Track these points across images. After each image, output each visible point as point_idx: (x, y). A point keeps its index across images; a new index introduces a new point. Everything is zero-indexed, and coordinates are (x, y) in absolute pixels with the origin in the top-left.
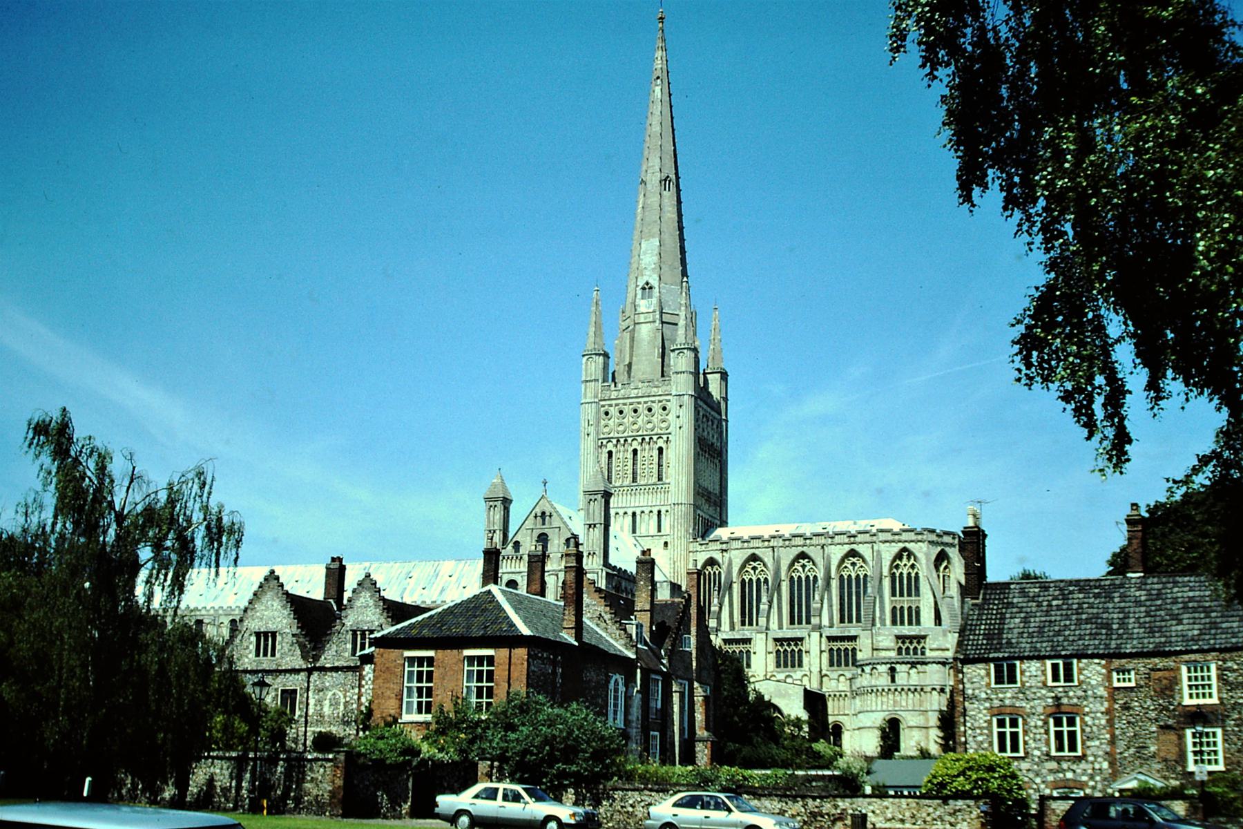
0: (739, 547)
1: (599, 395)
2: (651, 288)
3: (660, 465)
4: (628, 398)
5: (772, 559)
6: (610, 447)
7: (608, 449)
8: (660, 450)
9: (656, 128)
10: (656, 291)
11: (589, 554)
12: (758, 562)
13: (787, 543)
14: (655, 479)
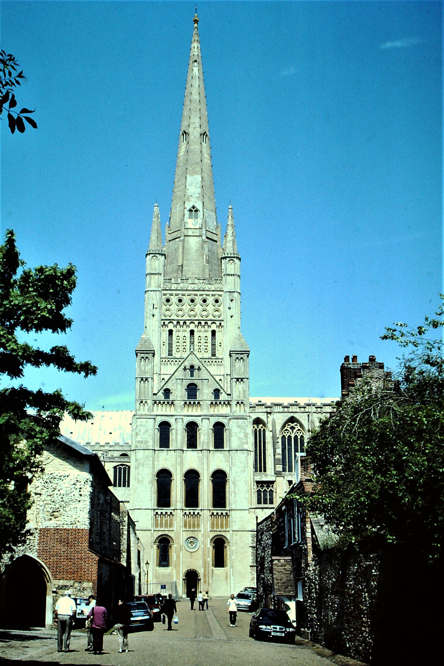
0: (281, 411)
1: (162, 286)
2: (196, 211)
3: (213, 345)
4: (187, 290)
5: (307, 421)
6: (171, 326)
7: (169, 328)
8: (214, 333)
9: (195, 96)
10: (200, 214)
11: (238, 403)
12: (296, 424)
13: (319, 410)
14: (209, 355)
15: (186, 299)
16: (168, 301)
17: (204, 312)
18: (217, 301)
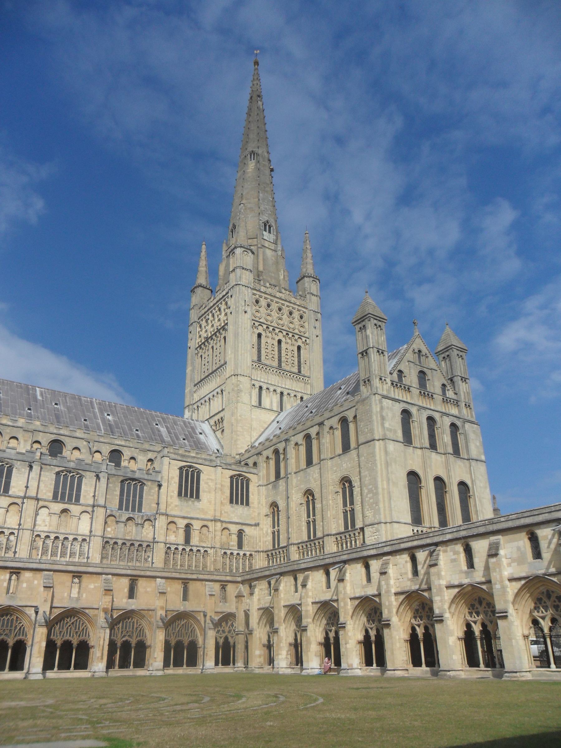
3: (299, 362)
6: (260, 330)
15: (274, 306)
16: (257, 302)
17: (291, 324)
18: (301, 317)
